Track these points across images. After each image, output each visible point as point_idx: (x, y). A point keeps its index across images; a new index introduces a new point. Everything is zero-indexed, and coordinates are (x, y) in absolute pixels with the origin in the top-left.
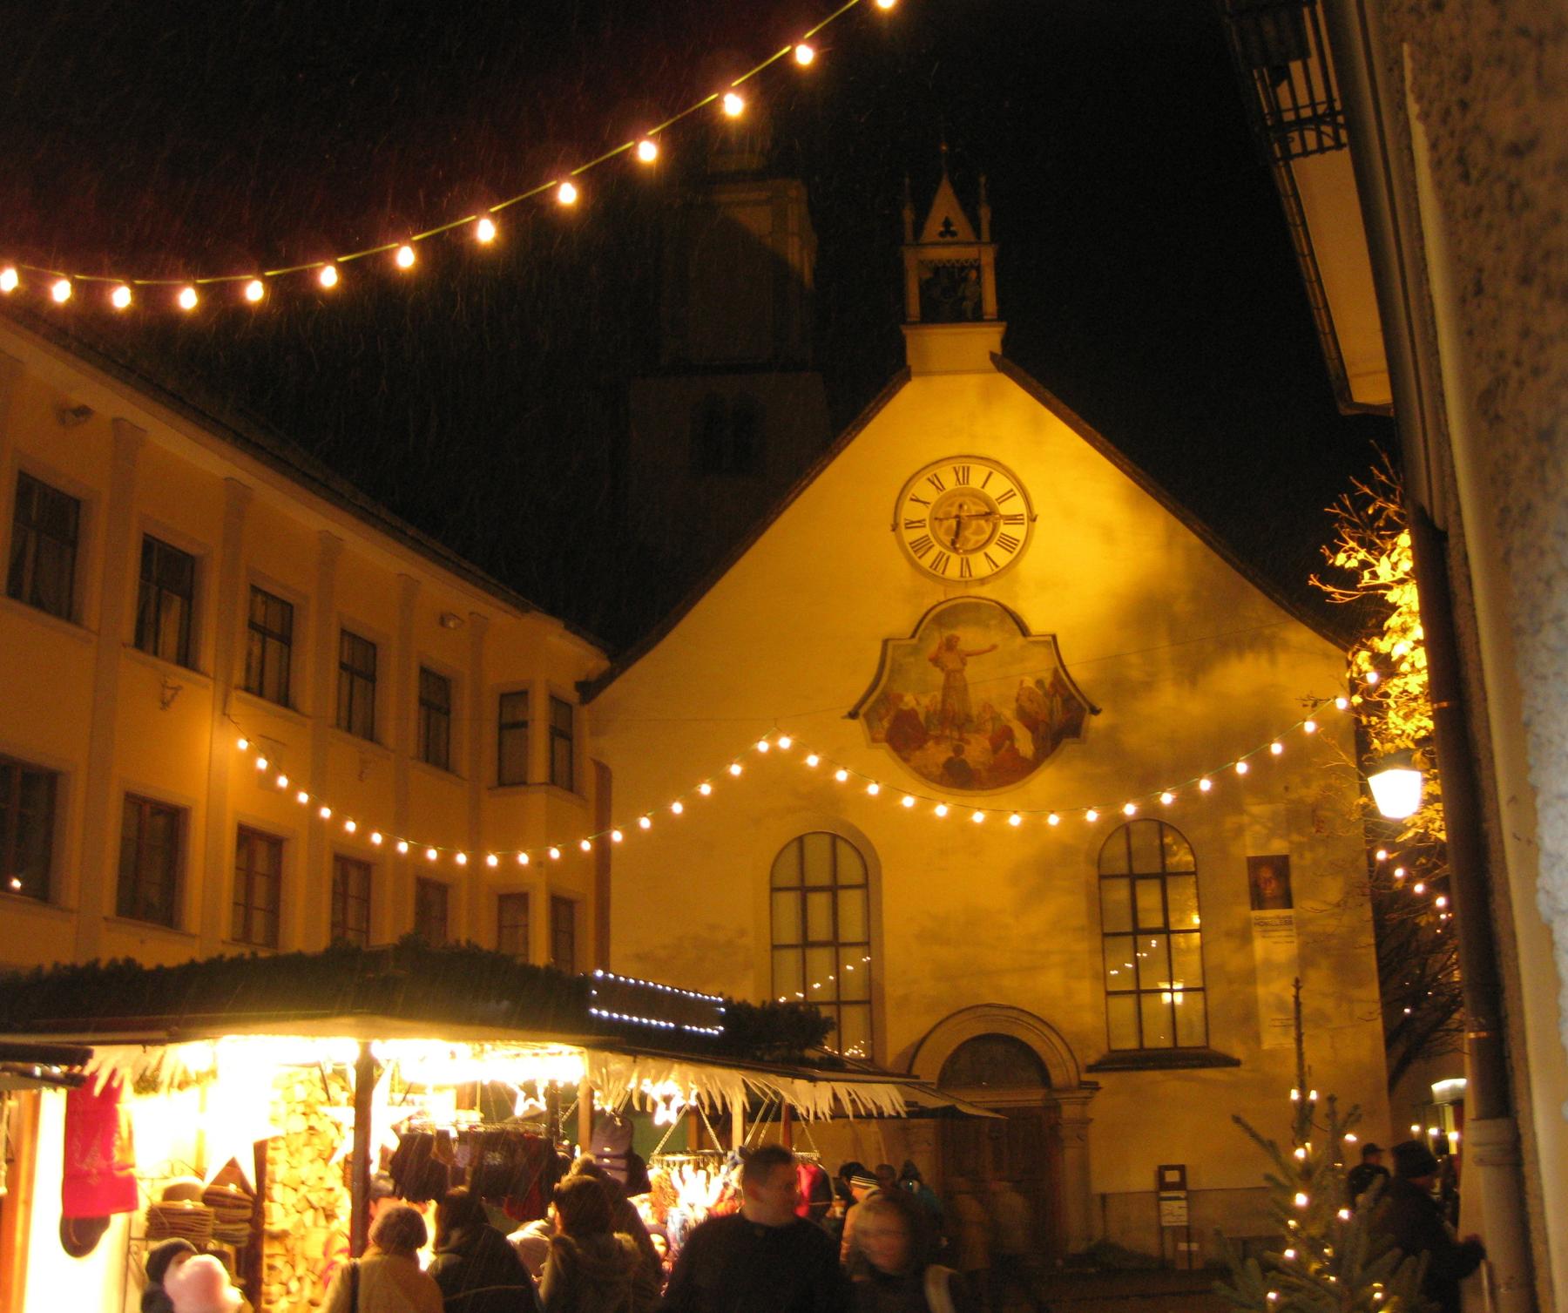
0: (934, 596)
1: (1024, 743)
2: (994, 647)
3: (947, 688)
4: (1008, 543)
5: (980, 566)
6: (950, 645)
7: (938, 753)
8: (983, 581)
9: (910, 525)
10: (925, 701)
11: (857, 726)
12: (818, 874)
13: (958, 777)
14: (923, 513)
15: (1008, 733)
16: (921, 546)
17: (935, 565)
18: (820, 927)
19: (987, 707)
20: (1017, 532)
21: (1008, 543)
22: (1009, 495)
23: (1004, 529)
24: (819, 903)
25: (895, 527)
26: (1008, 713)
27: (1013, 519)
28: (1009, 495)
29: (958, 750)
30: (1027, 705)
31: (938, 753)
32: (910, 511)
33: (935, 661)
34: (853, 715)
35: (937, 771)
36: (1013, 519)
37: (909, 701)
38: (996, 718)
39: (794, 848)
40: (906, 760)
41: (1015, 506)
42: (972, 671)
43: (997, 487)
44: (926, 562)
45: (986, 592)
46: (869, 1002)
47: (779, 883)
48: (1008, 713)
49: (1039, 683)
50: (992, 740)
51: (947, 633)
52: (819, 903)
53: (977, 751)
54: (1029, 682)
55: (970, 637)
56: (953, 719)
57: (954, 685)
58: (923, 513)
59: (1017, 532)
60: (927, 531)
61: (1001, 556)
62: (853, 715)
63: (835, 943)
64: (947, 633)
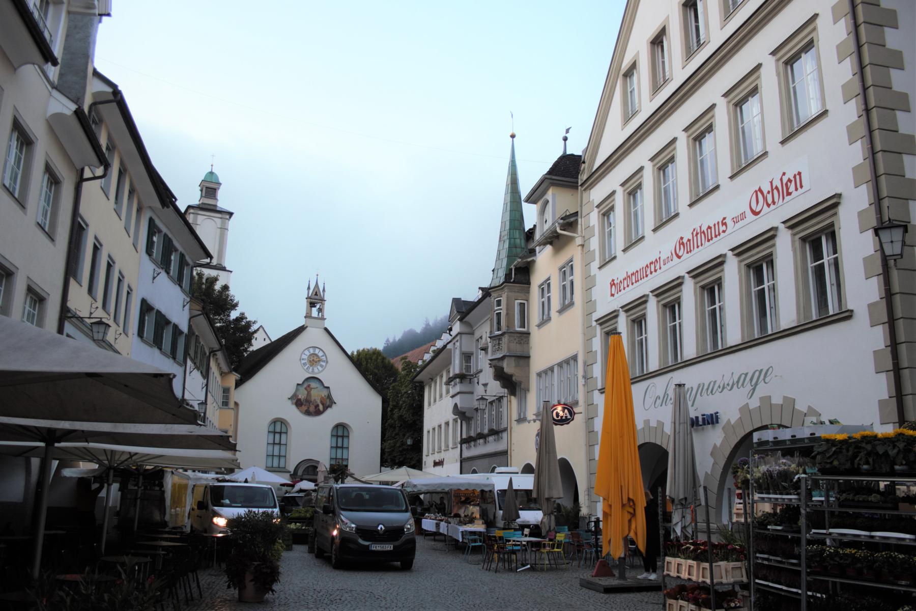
1: (321, 407)
4: (322, 366)
6: (309, 386)
7: (304, 408)
11: (290, 402)
13: (308, 413)
14: (305, 357)
15: (318, 406)
16: (305, 364)
18: (277, 441)
20: (324, 364)
21: (322, 366)
24: (277, 436)
31: (304, 408)
32: (304, 357)
37: (300, 397)
41: (324, 358)
42: (313, 392)
43: (321, 354)
52: (277, 436)
53: (312, 409)
55: (313, 384)
56: (308, 401)
57: (309, 394)
58: (305, 357)
59: (324, 364)
61: (320, 369)
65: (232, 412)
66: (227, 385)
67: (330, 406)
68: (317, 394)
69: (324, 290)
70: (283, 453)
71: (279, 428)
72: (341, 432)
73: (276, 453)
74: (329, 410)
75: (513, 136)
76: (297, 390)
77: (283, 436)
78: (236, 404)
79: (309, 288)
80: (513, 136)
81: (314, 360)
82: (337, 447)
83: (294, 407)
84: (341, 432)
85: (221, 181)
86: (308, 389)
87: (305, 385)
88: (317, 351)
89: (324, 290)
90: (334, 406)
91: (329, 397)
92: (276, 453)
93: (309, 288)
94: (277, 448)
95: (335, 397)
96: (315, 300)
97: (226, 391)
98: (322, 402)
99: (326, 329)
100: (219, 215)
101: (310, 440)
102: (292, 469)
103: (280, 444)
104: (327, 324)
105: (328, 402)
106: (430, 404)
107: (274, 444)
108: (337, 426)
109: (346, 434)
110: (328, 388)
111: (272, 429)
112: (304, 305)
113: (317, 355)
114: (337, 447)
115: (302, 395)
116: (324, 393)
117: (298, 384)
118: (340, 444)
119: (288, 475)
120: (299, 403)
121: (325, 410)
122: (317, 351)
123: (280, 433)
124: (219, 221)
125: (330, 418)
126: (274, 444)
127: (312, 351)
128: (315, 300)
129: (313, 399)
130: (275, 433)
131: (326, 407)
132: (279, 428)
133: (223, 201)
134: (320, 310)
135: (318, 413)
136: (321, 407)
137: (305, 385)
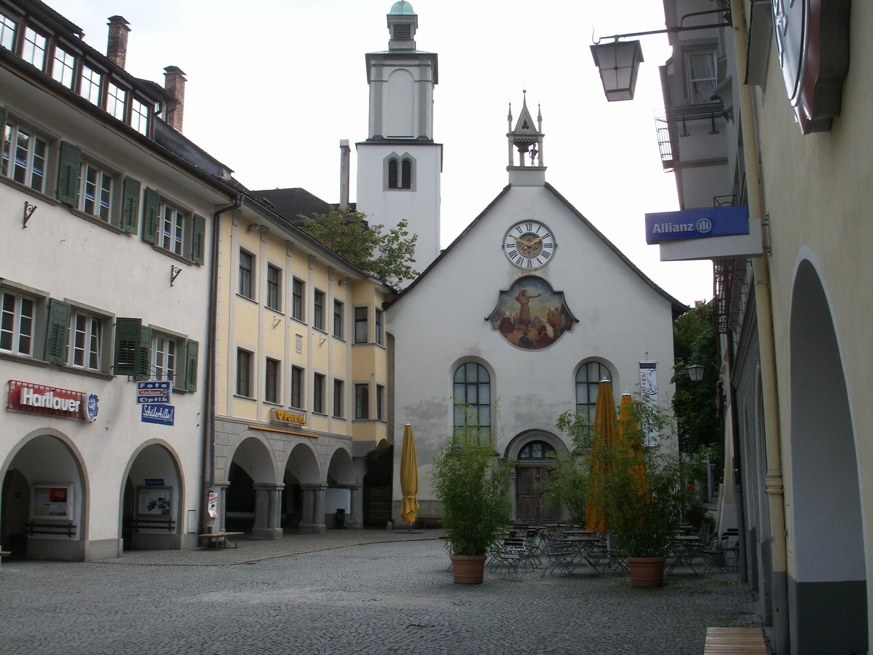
0: (519, 275)
1: (550, 331)
2: (540, 295)
3: (522, 310)
4: (546, 255)
5: (535, 264)
6: (523, 293)
7: (518, 335)
8: (536, 270)
9: (509, 246)
10: (513, 315)
11: (489, 325)
13: (525, 344)
15: (544, 328)
16: (513, 254)
17: (518, 262)
19: (537, 318)
20: (549, 250)
21: (546, 255)
22: (546, 236)
23: (545, 249)
24: (472, 391)
25: (503, 247)
26: (544, 320)
27: (549, 246)
28: (546, 236)
29: (526, 334)
30: (551, 317)
31: (518, 335)
33: (517, 299)
34: (487, 320)
35: (518, 342)
36: (549, 246)
38: (540, 322)
39: (463, 368)
40: (506, 337)
42: (532, 304)
43: (542, 233)
44: (515, 261)
45: (538, 274)
46: (490, 426)
47: (456, 381)
48: (544, 320)
49: (556, 309)
50: (538, 330)
51: (522, 289)
52: (472, 391)
53: (532, 335)
54: (553, 309)
55: (531, 290)
56: (524, 321)
57: (524, 308)
59: (549, 250)
60: (515, 249)
61: (544, 260)
62: (487, 320)
63: (477, 405)
64: (522, 289)
65: (380, 355)
66: (361, 303)
68: (540, 308)
69: (540, 119)
70: (484, 421)
74: (567, 335)
76: (501, 302)
77: (483, 390)
79: (510, 118)
81: (530, 244)
83: (497, 335)
85: (416, 12)
86: (523, 298)
87: (516, 293)
89: (540, 119)
91: (565, 310)
93: (510, 118)
96: (525, 136)
97: (361, 315)
99: (548, 187)
100: (417, 62)
102: (501, 451)
104: (549, 177)
108: (586, 365)
110: (561, 294)
113: (535, 236)
115: (512, 311)
116: (554, 304)
117: (502, 292)
122: (534, 229)
124: (415, 71)
126: (467, 405)
127: (524, 229)
128: (525, 136)
129: (533, 314)
131: (559, 332)
133: (423, 42)
135: (544, 341)
136: (550, 331)
137: (516, 293)
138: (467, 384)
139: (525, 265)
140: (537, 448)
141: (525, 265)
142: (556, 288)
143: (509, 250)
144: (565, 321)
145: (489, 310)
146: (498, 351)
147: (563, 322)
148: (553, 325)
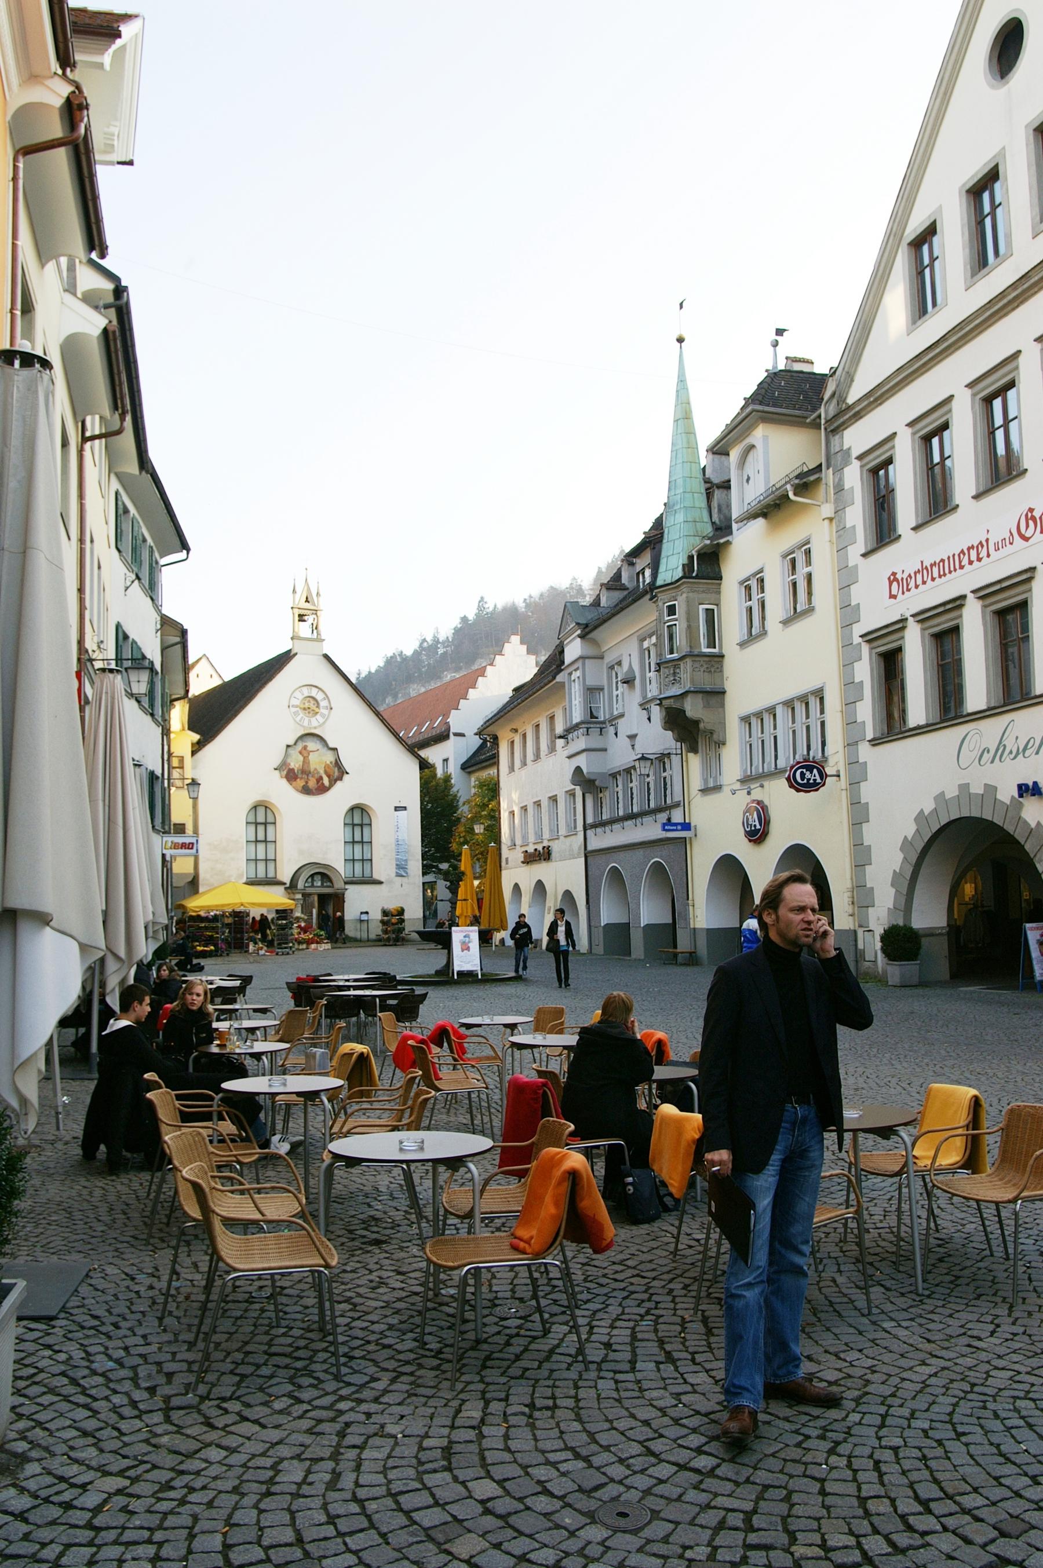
1: (326, 781)
4: (323, 715)
5: (314, 723)
6: (305, 748)
7: (300, 783)
12: (261, 819)
13: (306, 791)
15: (321, 778)
18: (261, 837)
21: (323, 715)
24: (261, 828)
31: (300, 783)
37: (292, 766)
42: (312, 757)
43: (320, 696)
44: (298, 719)
53: (312, 783)
55: (312, 745)
56: (305, 772)
57: (306, 761)
61: (321, 720)
63: (265, 841)
67: (340, 778)
68: (319, 760)
70: (271, 856)
71: (262, 817)
72: (359, 817)
73: (261, 855)
75: (680, 340)
76: (286, 755)
77: (270, 828)
78: (194, 783)
80: (680, 340)
81: (311, 706)
82: (354, 842)
84: (359, 817)
86: (305, 752)
88: (314, 692)
90: (346, 777)
91: (338, 764)
92: (261, 855)
94: (261, 847)
95: (346, 764)
98: (326, 772)
101: (310, 832)
103: (265, 841)
105: (338, 772)
106: (512, 769)
107: (257, 841)
108: (352, 809)
109: (366, 821)
111: (252, 819)
112: (289, 618)
114: (354, 842)
115: (296, 762)
116: (330, 758)
117: (288, 746)
118: (358, 838)
119: (281, 888)
120: (291, 776)
121: (331, 785)
123: (265, 824)
125: (341, 797)
126: (257, 841)
127: (306, 692)
130: (256, 824)
131: (333, 781)
132: (262, 817)
134: (315, 628)
135: (322, 789)
136: (326, 781)
138: (256, 824)
139: (306, 724)
140: (318, 878)
141: (306, 724)
142: (331, 745)
143: (293, 710)
144: (338, 772)
145: (277, 761)
146: (285, 798)
147: (336, 774)
148: (329, 776)
